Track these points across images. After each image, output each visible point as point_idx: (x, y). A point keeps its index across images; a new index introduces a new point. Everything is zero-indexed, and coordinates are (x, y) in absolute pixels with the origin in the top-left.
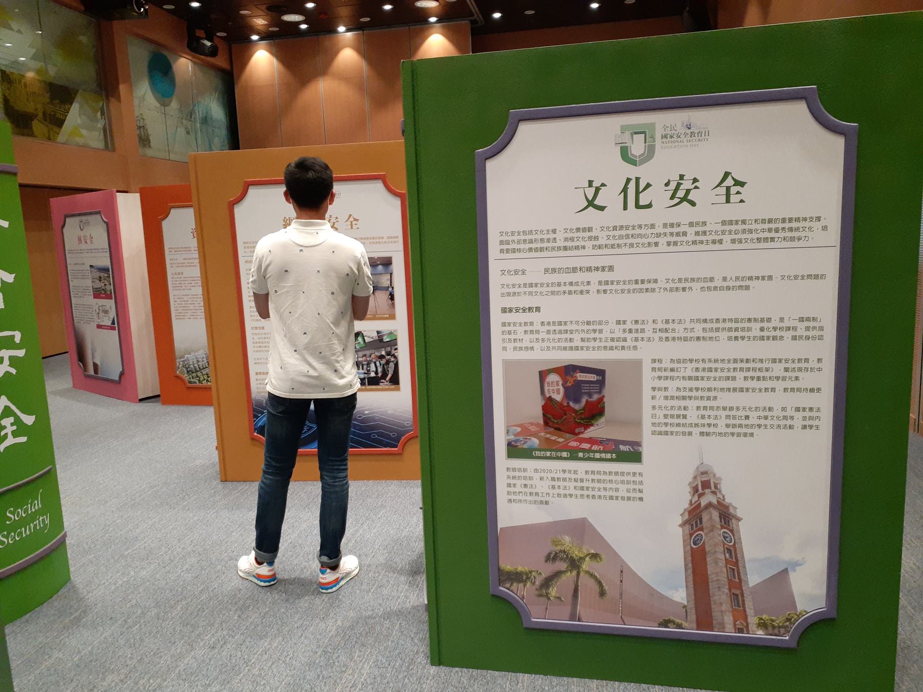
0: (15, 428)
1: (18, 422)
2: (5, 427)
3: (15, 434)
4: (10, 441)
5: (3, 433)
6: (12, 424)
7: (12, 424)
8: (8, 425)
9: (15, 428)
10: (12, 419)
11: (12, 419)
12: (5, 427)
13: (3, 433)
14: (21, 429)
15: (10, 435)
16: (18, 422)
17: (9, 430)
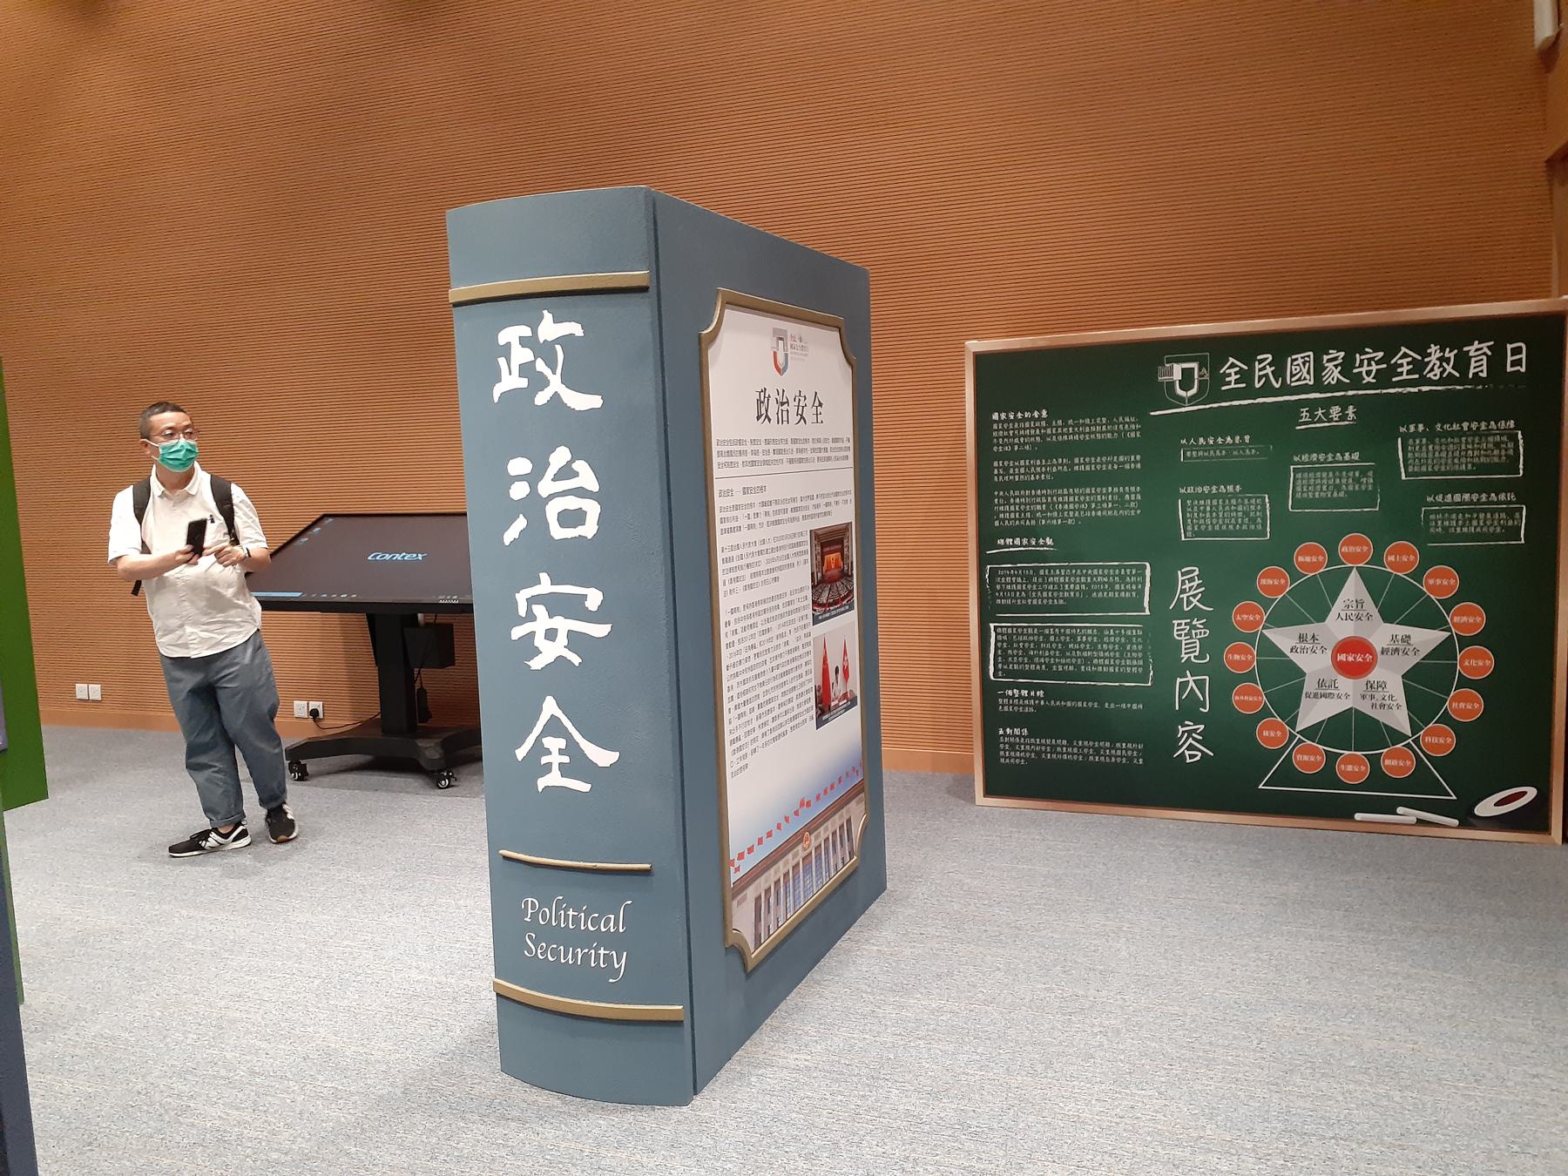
0: (566, 759)
1: (572, 749)
2: (548, 752)
3: (565, 770)
4: (554, 779)
5: (544, 760)
6: (561, 752)
7: (561, 752)
8: (555, 752)
9: (566, 759)
10: (562, 743)
11: (562, 743)
12: (548, 752)
13: (544, 760)
14: (577, 765)
15: (555, 767)
16: (572, 749)
17: (555, 759)
